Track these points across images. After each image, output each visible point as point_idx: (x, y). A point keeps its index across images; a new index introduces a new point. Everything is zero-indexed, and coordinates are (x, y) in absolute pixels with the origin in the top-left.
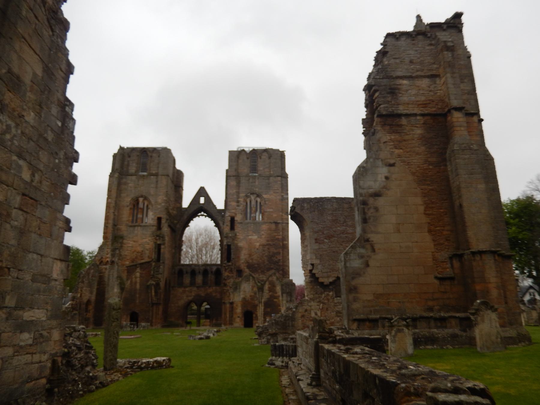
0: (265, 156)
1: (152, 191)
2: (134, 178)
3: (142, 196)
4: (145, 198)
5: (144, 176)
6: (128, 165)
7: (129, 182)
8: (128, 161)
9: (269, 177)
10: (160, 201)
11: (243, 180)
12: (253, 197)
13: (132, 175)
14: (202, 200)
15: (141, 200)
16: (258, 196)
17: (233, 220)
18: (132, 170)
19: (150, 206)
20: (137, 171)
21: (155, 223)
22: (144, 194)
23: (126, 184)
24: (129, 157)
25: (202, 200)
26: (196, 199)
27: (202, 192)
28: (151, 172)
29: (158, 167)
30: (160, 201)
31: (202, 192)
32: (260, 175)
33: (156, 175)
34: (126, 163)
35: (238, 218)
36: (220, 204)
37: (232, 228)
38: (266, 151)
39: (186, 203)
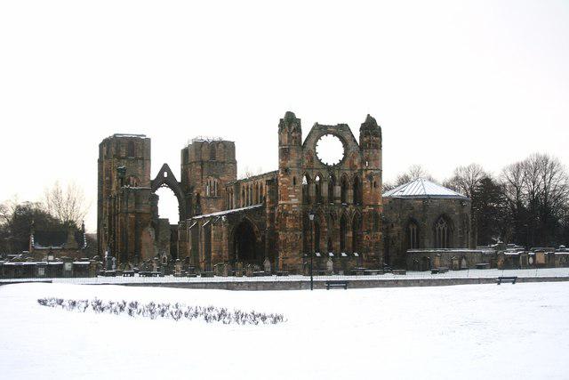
0: (221, 146)
9: (223, 163)
11: (206, 165)
12: (212, 179)
13: (123, 158)
14: (166, 175)
16: (217, 177)
17: (198, 194)
25: (166, 175)
26: (161, 173)
27: (165, 168)
31: (165, 168)
32: (218, 161)
33: (142, 159)
35: (202, 194)
36: (179, 179)
37: (198, 202)
38: (222, 142)
39: (153, 176)
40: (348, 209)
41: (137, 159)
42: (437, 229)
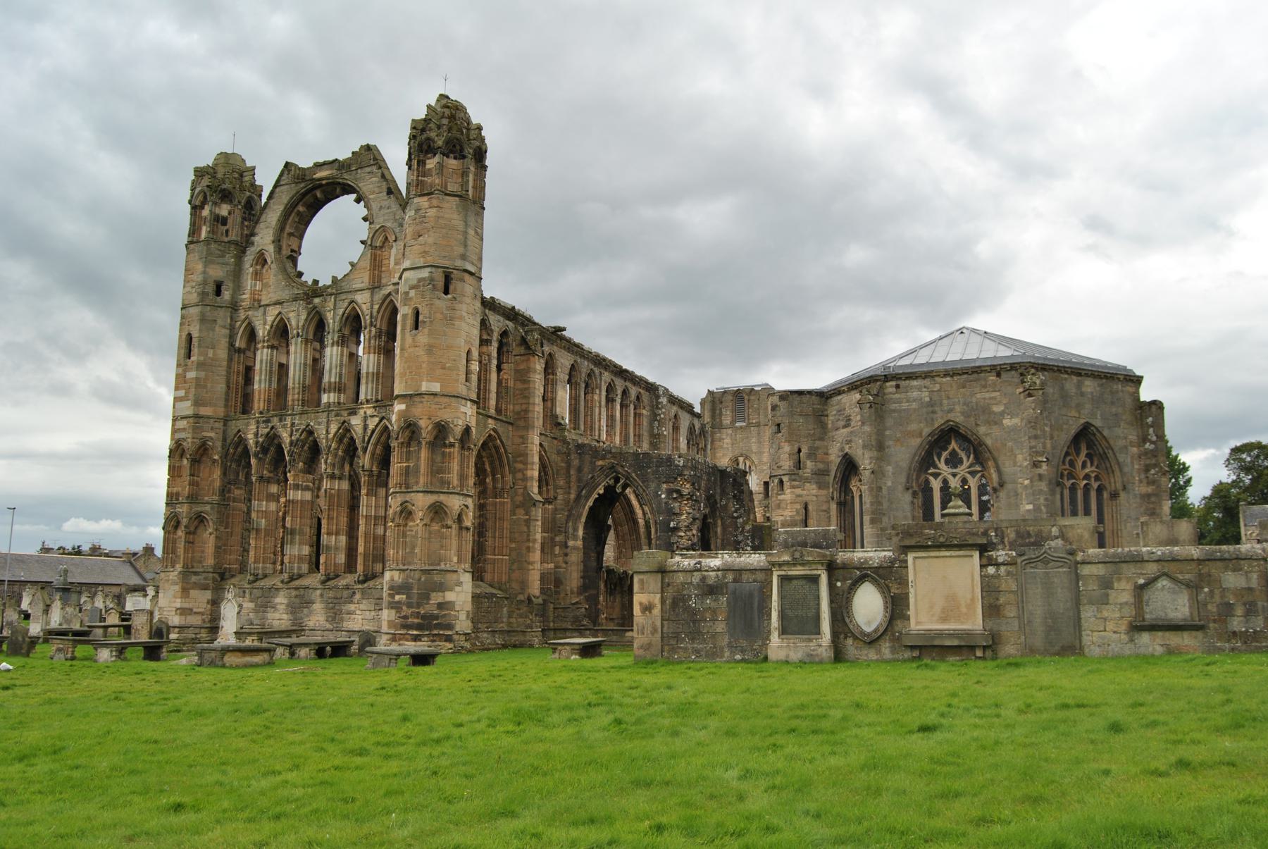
1: (754, 447)
2: (730, 431)
3: (742, 456)
4: (747, 457)
5: (741, 427)
6: (721, 414)
7: (724, 437)
8: (720, 409)
10: (765, 459)
15: (741, 459)
18: (727, 420)
19: (753, 468)
20: (733, 422)
21: (762, 489)
22: (744, 452)
23: (721, 439)
24: (721, 402)
28: (751, 421)
29: (759, 414)
30: (765, 459)
33: (758, 425)
34: (718, 412)
40: (356, 421)
41: (749, 425)
42: (936, 484)
